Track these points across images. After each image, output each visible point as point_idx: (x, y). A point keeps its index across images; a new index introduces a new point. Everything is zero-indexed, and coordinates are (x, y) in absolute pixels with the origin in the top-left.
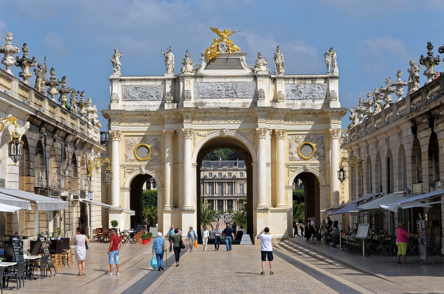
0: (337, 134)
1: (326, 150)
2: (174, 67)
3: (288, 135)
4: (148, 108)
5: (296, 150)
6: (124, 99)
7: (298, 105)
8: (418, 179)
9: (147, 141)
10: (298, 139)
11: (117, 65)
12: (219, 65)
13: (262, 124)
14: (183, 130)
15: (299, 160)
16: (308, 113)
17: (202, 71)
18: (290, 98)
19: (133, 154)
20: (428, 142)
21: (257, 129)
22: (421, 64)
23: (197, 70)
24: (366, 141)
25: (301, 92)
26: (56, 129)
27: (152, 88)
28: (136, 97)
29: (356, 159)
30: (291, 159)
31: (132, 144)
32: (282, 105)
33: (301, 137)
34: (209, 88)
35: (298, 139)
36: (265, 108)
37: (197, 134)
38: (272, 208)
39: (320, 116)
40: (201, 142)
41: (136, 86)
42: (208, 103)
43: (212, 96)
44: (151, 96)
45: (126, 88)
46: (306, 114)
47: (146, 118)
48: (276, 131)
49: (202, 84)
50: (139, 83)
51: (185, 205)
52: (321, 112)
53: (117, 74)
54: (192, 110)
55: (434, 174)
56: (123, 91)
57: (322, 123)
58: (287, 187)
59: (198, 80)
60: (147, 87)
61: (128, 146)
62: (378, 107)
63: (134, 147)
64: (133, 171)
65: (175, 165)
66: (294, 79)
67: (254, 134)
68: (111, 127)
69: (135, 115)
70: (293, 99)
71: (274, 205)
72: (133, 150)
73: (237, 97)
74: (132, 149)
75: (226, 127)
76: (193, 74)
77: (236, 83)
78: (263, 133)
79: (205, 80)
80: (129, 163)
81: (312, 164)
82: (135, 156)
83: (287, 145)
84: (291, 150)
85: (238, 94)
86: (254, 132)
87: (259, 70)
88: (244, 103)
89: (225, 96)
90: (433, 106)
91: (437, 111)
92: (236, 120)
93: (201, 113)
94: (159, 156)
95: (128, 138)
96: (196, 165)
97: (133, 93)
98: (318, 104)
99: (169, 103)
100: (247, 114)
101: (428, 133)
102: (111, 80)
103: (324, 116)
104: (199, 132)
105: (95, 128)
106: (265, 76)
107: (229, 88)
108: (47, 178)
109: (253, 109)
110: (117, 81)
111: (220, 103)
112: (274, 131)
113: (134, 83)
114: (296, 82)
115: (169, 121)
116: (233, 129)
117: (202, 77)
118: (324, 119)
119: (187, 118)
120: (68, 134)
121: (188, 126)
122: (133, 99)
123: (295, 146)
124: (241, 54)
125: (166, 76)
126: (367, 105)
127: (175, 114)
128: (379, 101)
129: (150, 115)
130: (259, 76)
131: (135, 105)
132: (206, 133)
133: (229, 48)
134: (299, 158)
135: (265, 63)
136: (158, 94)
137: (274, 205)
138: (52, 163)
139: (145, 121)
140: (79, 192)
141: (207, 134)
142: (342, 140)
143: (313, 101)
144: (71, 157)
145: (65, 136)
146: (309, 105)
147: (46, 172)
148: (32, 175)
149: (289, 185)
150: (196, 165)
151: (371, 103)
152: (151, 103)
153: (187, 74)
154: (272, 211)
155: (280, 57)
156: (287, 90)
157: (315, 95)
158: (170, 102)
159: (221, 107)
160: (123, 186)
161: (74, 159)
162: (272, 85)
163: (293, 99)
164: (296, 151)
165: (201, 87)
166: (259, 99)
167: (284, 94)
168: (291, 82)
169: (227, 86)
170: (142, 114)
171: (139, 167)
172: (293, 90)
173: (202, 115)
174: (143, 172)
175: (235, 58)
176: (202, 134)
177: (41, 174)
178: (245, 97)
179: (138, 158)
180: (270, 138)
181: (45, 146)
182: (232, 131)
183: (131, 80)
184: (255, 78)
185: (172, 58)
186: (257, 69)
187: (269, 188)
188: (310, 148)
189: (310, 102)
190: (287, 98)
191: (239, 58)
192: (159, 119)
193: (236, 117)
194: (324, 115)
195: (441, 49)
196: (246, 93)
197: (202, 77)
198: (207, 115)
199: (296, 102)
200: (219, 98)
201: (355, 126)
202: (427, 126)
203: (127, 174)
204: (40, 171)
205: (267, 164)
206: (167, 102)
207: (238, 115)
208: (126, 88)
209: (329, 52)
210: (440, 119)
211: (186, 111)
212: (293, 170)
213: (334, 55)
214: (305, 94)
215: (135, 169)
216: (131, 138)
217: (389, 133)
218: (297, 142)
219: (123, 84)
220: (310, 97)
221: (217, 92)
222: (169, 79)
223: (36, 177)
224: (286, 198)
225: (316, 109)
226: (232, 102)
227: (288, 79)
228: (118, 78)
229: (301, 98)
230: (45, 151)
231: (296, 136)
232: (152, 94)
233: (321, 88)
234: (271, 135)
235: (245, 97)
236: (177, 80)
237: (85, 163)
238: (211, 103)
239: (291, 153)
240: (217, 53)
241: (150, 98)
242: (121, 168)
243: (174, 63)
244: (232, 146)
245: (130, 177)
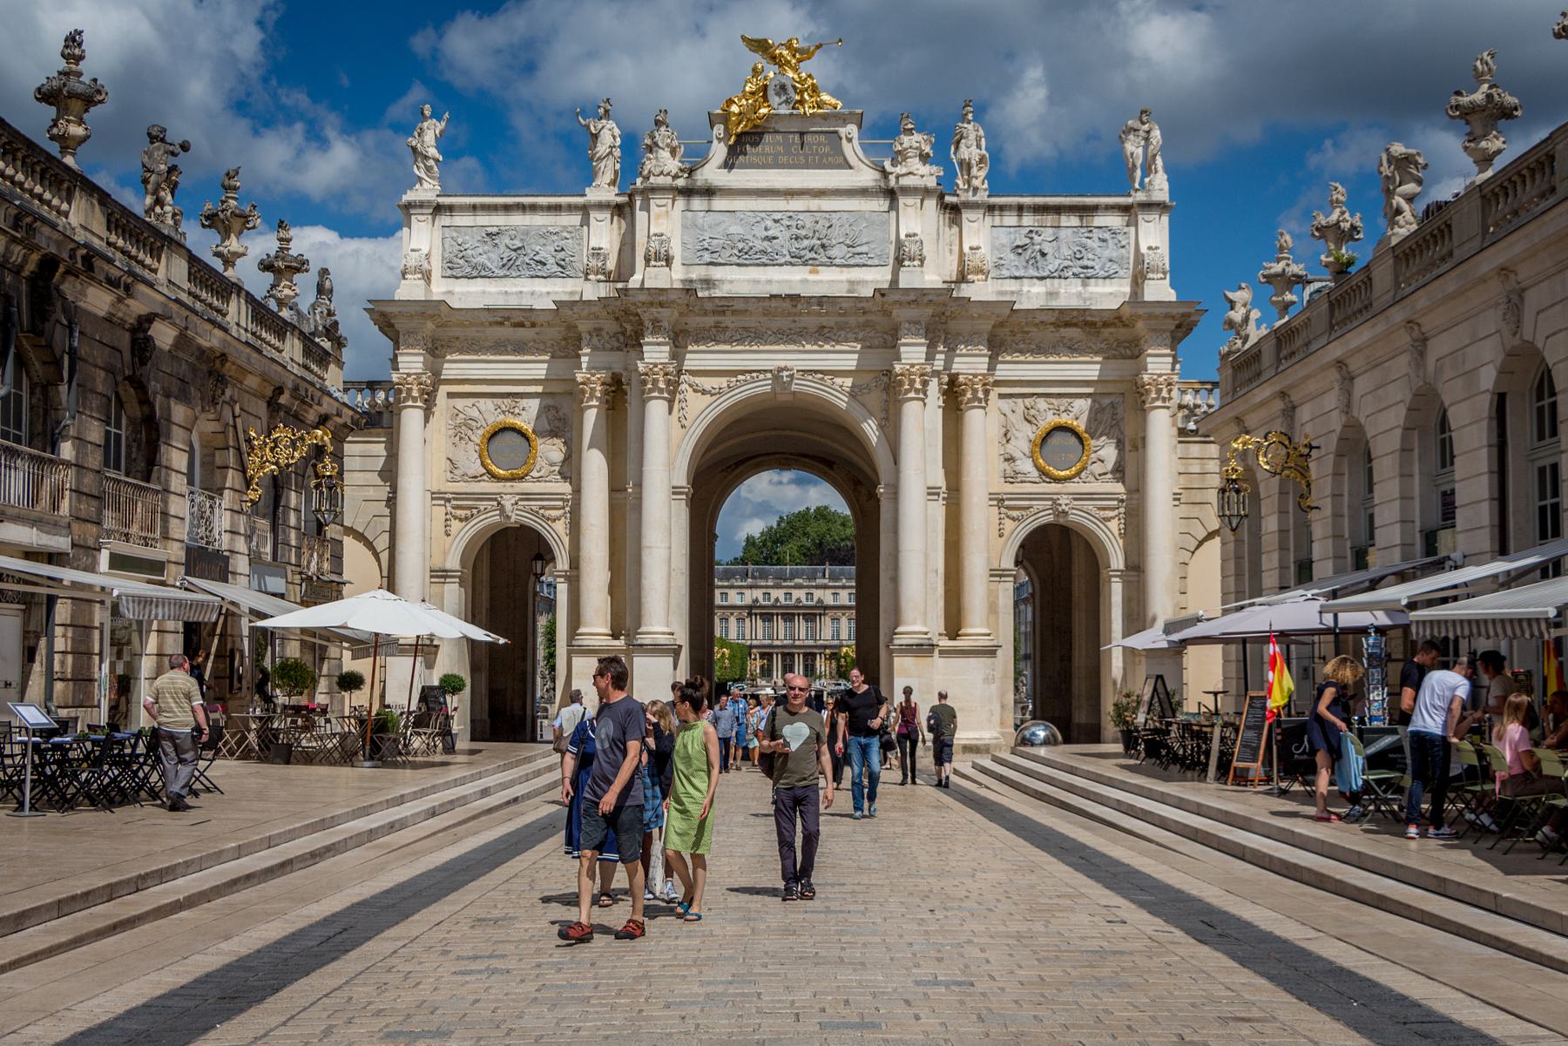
0: (1170, 391)
1: (1128, 447)
2: (618, 166)
3: (1001, 396)
4: (526, 302)
5: (1026, 447)
6: (449, 272)
7: (1033, 295)
9: (524, 413)
10: (1032, 412)
11: (426, 157)
12: (768, 155)
13: (912, 353)
14: (641, 367)
15: (1038, 480)
16: (1067, 325)
17: (712, 173)
18: (1006, 273)
19: (476, 455)
21: (898, 368)
23: (691, 171)
24: (1340, 364)
25: (1043, 255)
27: (546, 235)
28: (489, 265)
29: (1287, 443)
30: (1010, 479)
31: (474, 424)
32: (980, 291)
33: (1042, 404)
34: (735, 229)
35: (1032, 412)
36: (923, 292)
37: (690, 386)
38: (945, 643)
39: (1106, 332)
41: (490, 230)
42: (731, 282)
43: (746, 257)
44: (541, 262)
45: (455, 234)
46: (1059, 326)
47: (522, 333)
48: (961, 379)
49: (711, 217)
50: (499, 220)
51: (642, 629)
52: (1115, 319)
53: (426, 190)
54: (673, 297)
56: (447, 246)
57: (1115, 357)
59: (698, 203)
60: (527, 233)
61: (461, 429)
62: (1408, 214)
63: (480, 432)
64: (475, 511)
65: (618, 495)
66: (1020, 209)
67: (887, 389)
68: (400, 359)
69: (482, 324)
70: (1016, 278)
71: (954, 626)
72: (478, 441)
73: (831, 263)
74: (473, 438)
75: (789, 364)
76: (681, 182)
77: (827, 215)
78: (918, 380)
79: (719, 203)
80: (462, 487)
81: (1079, 497)
82: (483, 464)
83: (995, 431)
84: (1008, 446)
85: (833, 252)
86: (885, 379)
87: (904, 171)
88: (851, 283)
89: (788, 258)
92: (827, 340)
93: (705, 314)
95: (460, 403)
96: (686, 494)
97: (480, 250)
98: (1102, 295)
99: (599, 281)
100: (862, 319)
102: (409, 206)
103: (1123, 333)
104: (698, 380)
105: (322, 344)
106: (926, 192)
107: (803, 232)
109: (883, 295)
110: (425, 211)
111: (769, 282)
113: (483, 219)
114: (1028, 220)
115: (595, 340)
116: (816, 372)
117: (709, 192)
118: (1120, 343)
119: (657, 328)
121: (658, 355)
122: (479, 272)
123: (1024, 436)
124: (844, 119)
125: (593, 195)
127: (617, 319)
128: (1410, 187)
129: (533, 325)
130: (907, 191)
131: (484, 292)
132: (722, 382)
133: (802, 96)
134: (1035, 473)
135: (927, 149)
136: (562, 255)
137: (954, 626)
139: (520, 348)
140: (175, 552)
141: (725, 385)
142: (1180, 415)
143: (1084, 285)
145: (31, 267)
146: (1070, 295)
148: (176, 537)
149: (1003, 567)
150: (686, 494)
151: (1348, 225)
152: (541, 286)
154: (945, 653)
155: (972, 136)
156: (994, 248)
157: (1090, 263)
158: (602, 278)
159: (774, 293)
160: (438, 564)
161: (146, 409)
162: (947, 229)
163: (1016, 278)
164: (1027, 451)
165: (706, 227)
166: (906, 263)
167: (988, 258)
168: (1011, 219)
169: (794, 223)
170: (508, 319)
171: (495, 500)
172: (1018, 247)
173: (710, 321)
174: (508, 517)
175: (822, 132)
176: (708, 388)
178: (857, 260)
179: (494, 468)
180: (941, 403)
182: (810, 378)
183: (474, 208)
184: (891, 194)
185: (614, 137)
186: (899, 170)
187: (936, 572)
188: (1073, 440)
189: (1075, 286)
190: (998, 272)
191: (836, 132)
192: (565, 339)
193: (826, 330)
194: (1122, 330)
196: (859, 249)
197: (709, 192)
198: (727, 320)
199: (1026, 286)
200: (766, 265)
201: (1247, 346)
203: (456, 525)
205: (932, 492)
206: (591, 277)
207: (832, 324)
208: (455, 234)
209: (1137, 124)
211: (652, 304)
212: (1015, 514)
213: (1152, 134)
214: (1057, 262)
215: (482, 508)
216: (471, 401)
217: (1524, 273)
218: (1029, 422)
219: (445, 220)
220: (1075, 270)
221: (759, 245)
222: (601, 206)
224: (993, 609)
225: (1093, 307)
226: (811, 277)
227: (1002, 208)
228: (428, 202)
229: (1045, 274)
231: (1028, 401)
232: (543, 254)
233: (1110, 242)
234: (944, 393)
235: (857, 260)
236: (627, 209)
237: (231, 443)
238: (738, 281)
239: (1010, 459)
240: (763, 111)
241: (537, 268)
242: (434, 502)
243: (617, 152)
244: (813, 458)
245: (463, 534)
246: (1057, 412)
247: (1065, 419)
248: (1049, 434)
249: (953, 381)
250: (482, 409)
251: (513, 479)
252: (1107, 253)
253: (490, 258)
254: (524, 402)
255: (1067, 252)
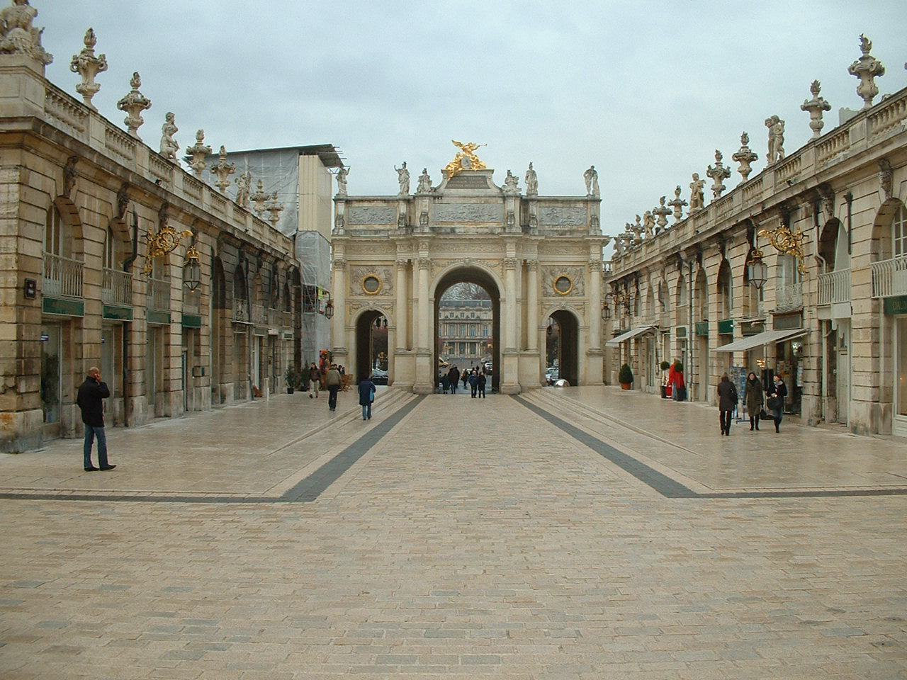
8: (702, 318)
20: (718, 272)
22: (709, 176)
26: (262, 252)
33: (557, 270)
40: (440, 273)
48: (528, 262)
55: (750, 305)
58: (540, 328)
61: (354, 278)
90: (727, 226)
91: (730, 233)
94: (390, 290)
101: (718, 261)
108: (249, 311)
112: (525, 261)
120: (277, 260)
123: (551, 280)
126: (638, 230)
138: (256, 294)
144: (281, 286)
147: (248, 304)
153: (425, 193)
177: (240, 307)
178: (492, 220)
181: (247, 273)
184: (504, 198)
195: (736, 157)
197: (440, 197)
202: (717, 252)
204: (240, 303)
210: (734, 244)
216: (358, 268)
223: (234, 309)
230: (246, 278)
239: (545, 288)
240: (460, 169)
246: (562, 272)
247: (564, 274)
248: (559, 280)
249: (525, 261)
250: (362, 270)
251: (372, 295)
252: (579, 217)
253: (366, 217)
254: (377, 268)
255: (565, 216)
